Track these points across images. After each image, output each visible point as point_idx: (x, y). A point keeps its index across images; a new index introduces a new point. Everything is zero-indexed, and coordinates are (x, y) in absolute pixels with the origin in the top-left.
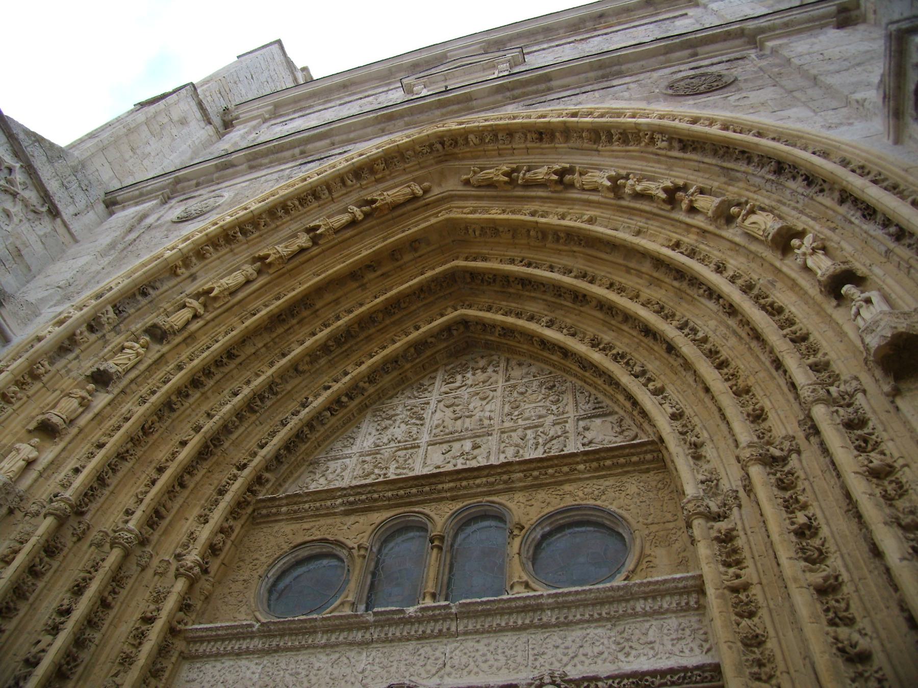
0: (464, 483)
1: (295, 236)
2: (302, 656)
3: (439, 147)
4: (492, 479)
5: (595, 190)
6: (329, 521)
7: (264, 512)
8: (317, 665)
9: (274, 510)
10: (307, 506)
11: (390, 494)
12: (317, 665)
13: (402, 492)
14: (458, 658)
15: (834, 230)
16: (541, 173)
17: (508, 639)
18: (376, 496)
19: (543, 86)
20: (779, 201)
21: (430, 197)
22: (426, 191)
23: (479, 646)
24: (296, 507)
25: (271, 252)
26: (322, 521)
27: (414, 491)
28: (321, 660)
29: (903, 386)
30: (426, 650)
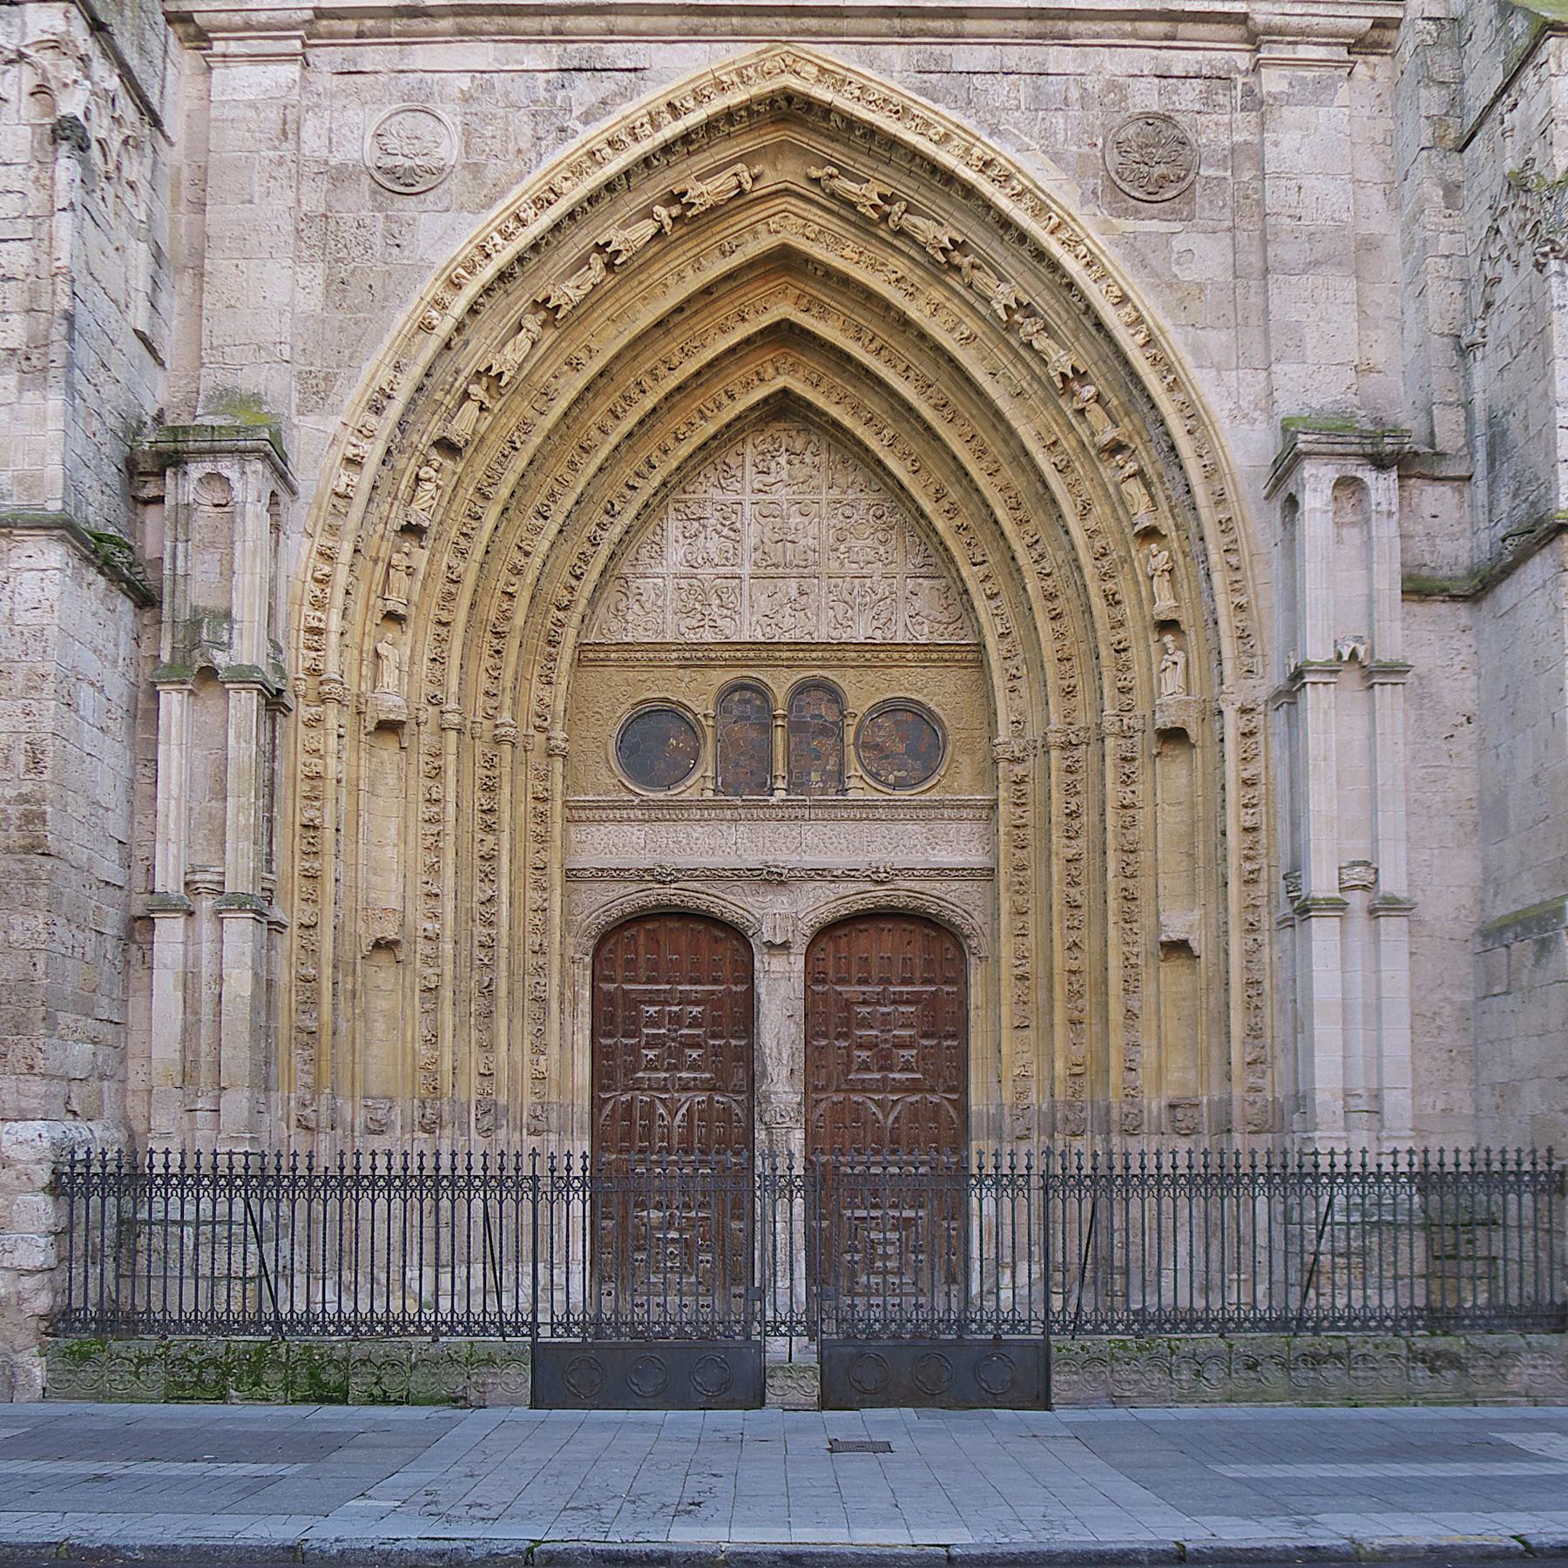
0: (801, 655)
1: (583, 261)
2: (680, 826)
3: (783, 104)
4: (827, 655)
5: (987, 300)
6: (666, 673)
7: (591, 655)
8: (695, 835)
9: (602, 655)
10: (639, 655)
11: (726, 655)
12: (695, 835)
13: (739, 654)
14: (810, 838)
15: (1185, 554)
16: (925, 228)
17: (849, 826)
18: (713, 655)
19: (948, 25)
20: (1160, 476)
21: (762, 188)
22: (755, 179)
23: (828, 830)
24: (626, 655)
25: (562, 302)
26: (657, 673)
27: (751, 654)
28: (697, 831)
29: (1165, 751)
30: (783, 828)
